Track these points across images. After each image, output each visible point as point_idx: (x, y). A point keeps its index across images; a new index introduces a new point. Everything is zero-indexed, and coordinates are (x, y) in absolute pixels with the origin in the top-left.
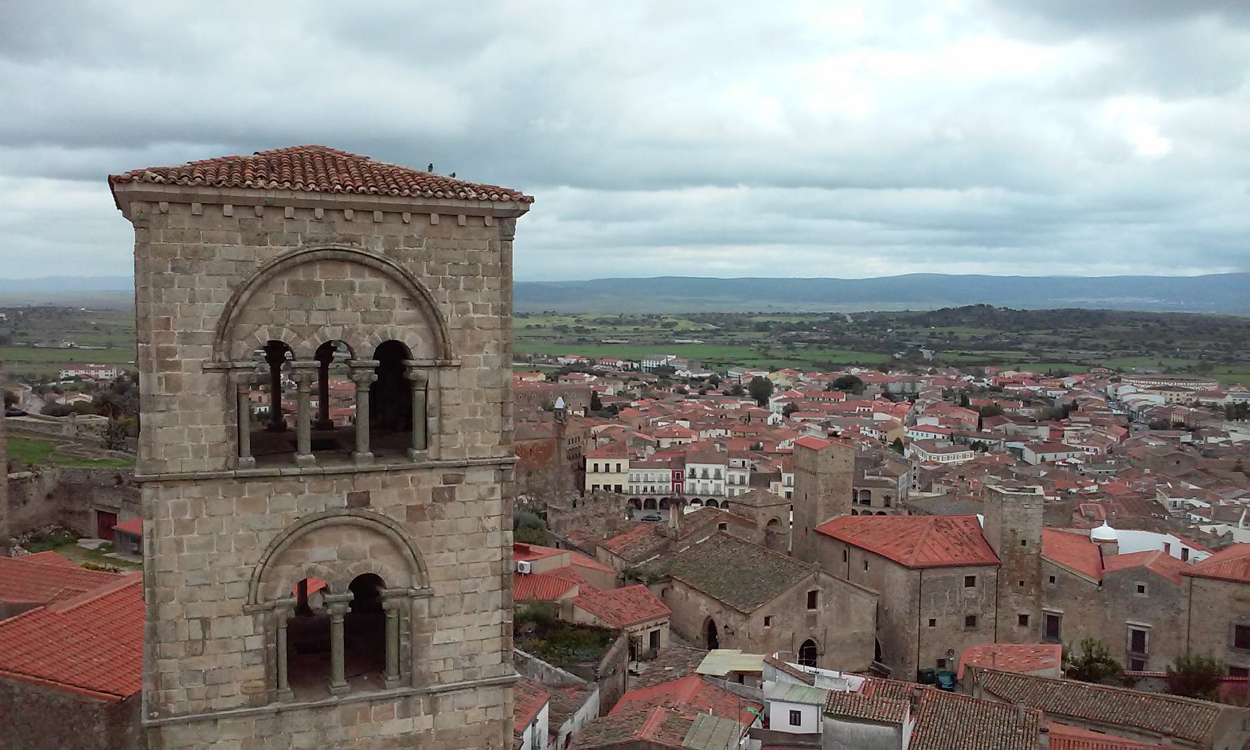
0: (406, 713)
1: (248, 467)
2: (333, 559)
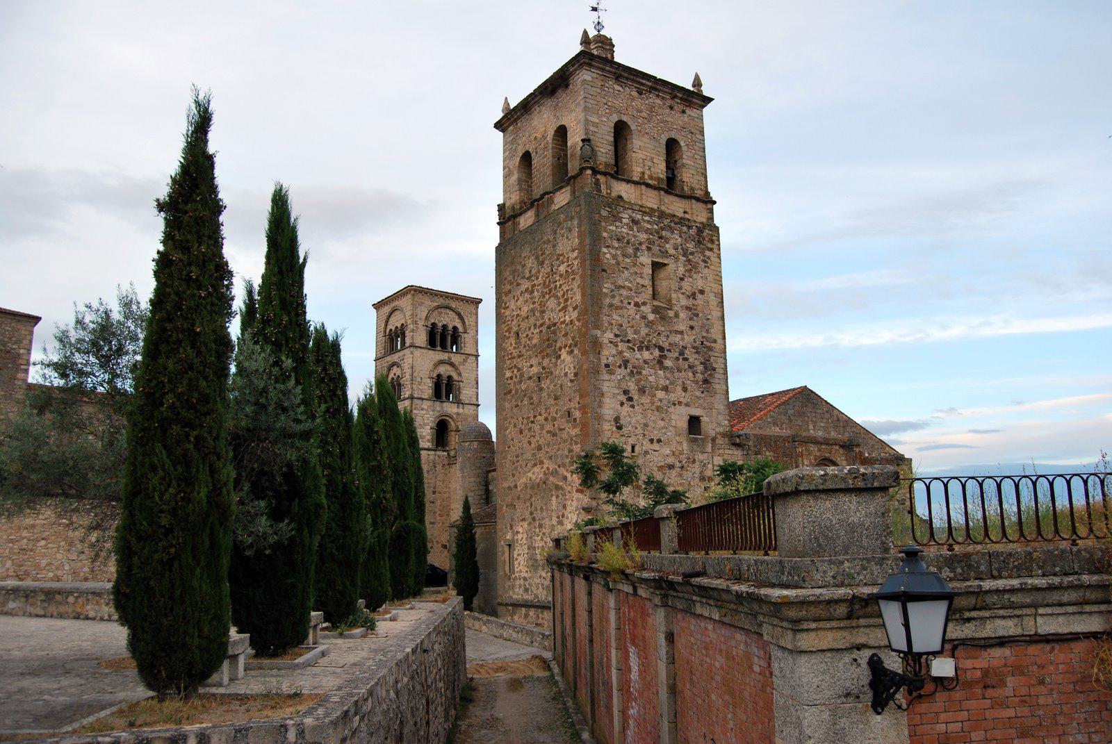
0: (458, 407)
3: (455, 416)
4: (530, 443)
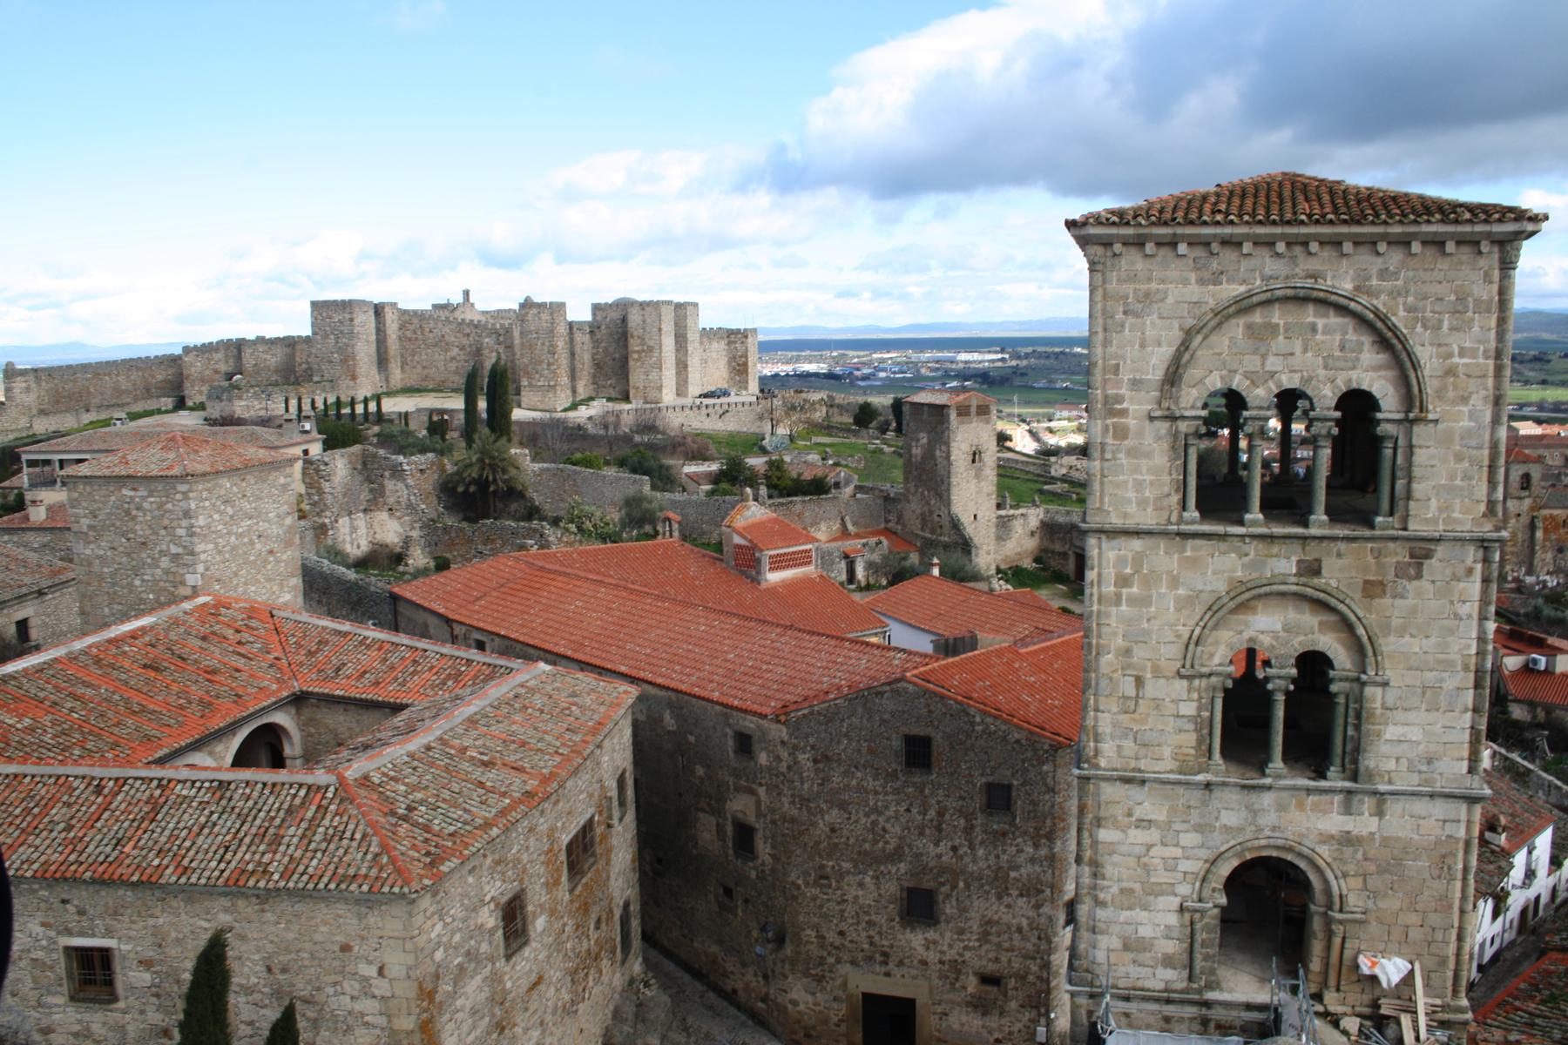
0: (1347, 810)
1: (1193, 522)
2: (1280, 631)
3: (1324, 851)
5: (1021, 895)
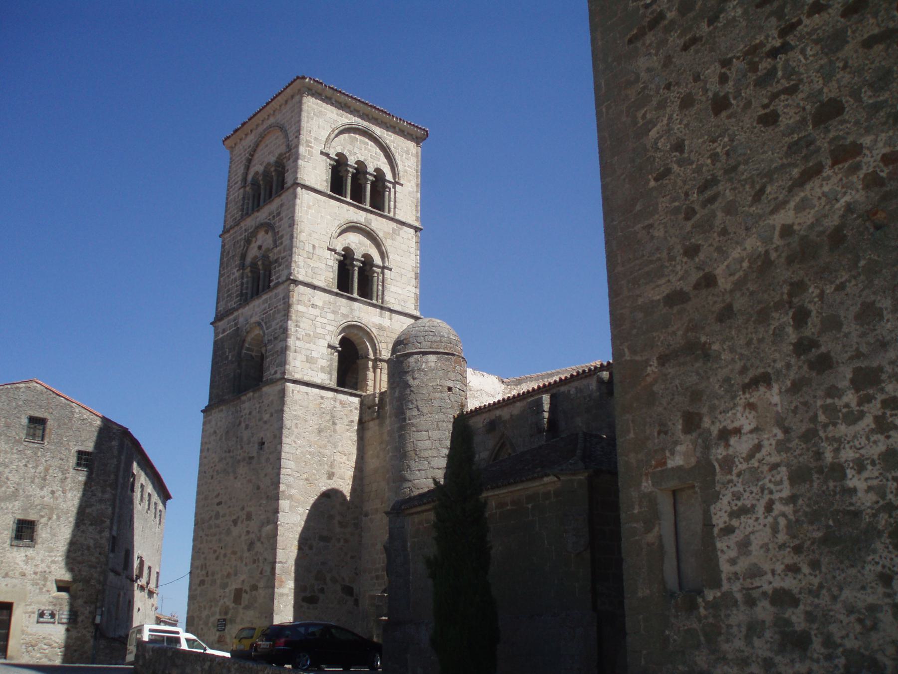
0: (381, 315)
3: (374, 330)
4: (770, 119)
5: (91, 524)
